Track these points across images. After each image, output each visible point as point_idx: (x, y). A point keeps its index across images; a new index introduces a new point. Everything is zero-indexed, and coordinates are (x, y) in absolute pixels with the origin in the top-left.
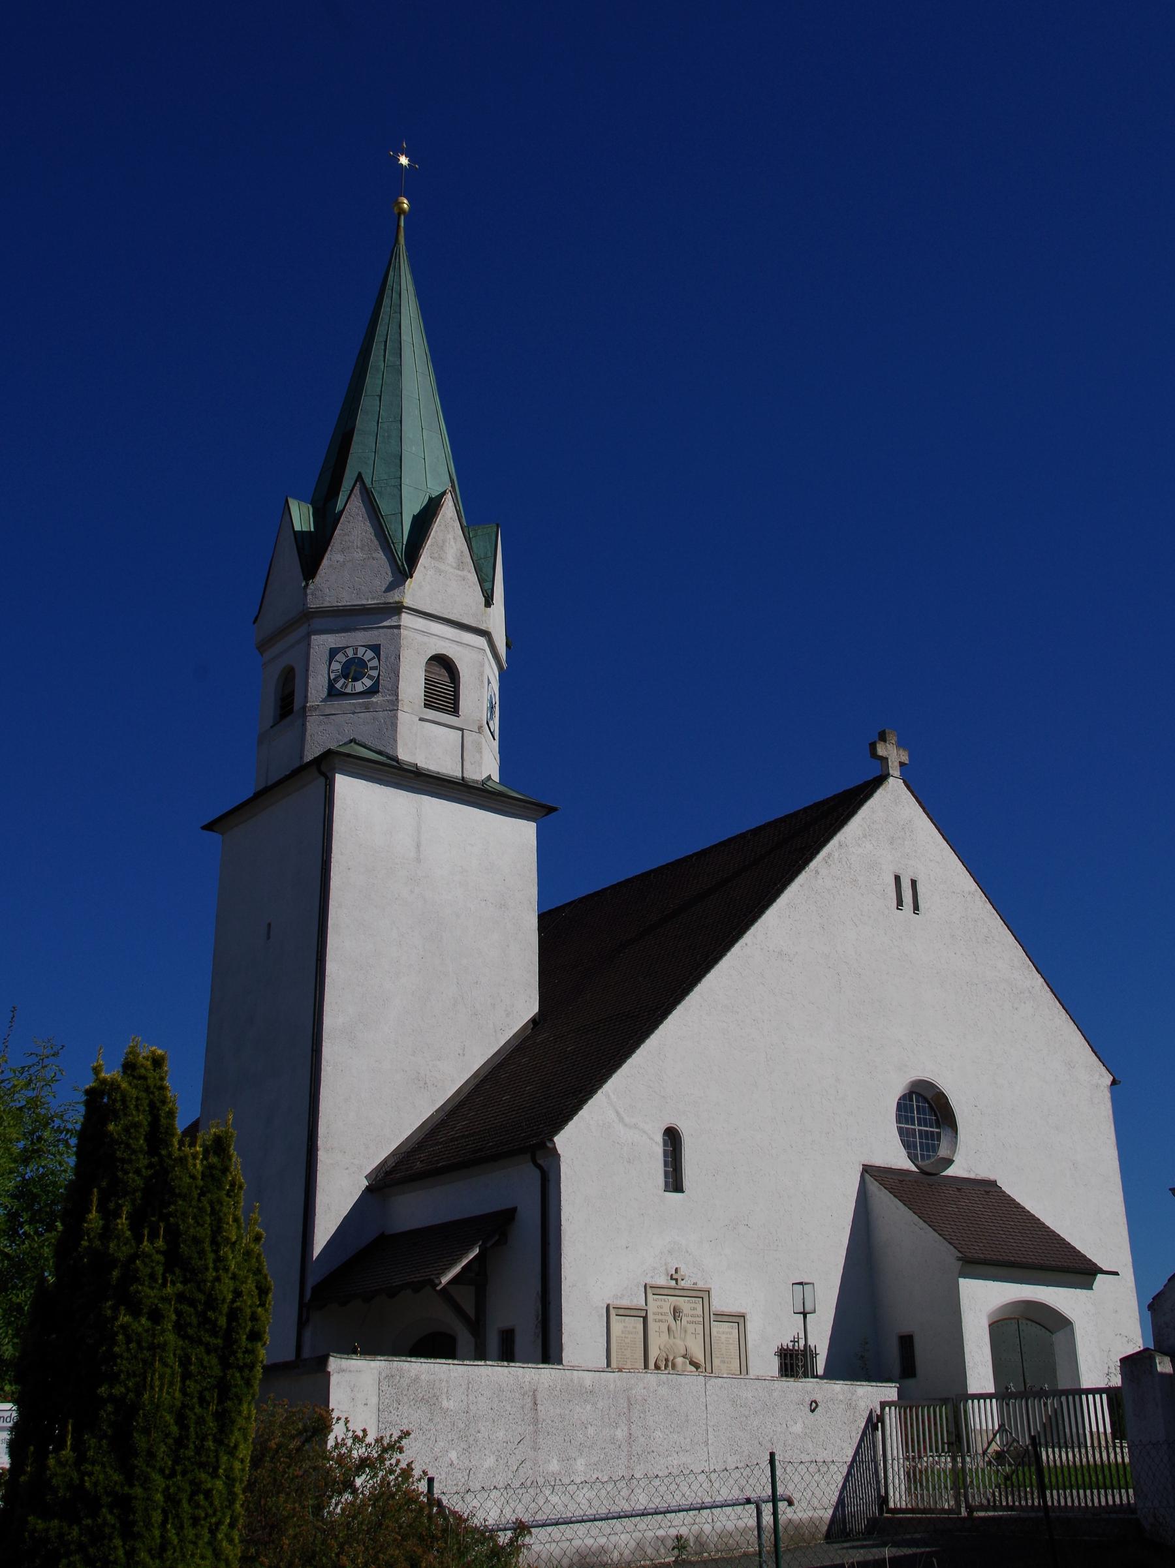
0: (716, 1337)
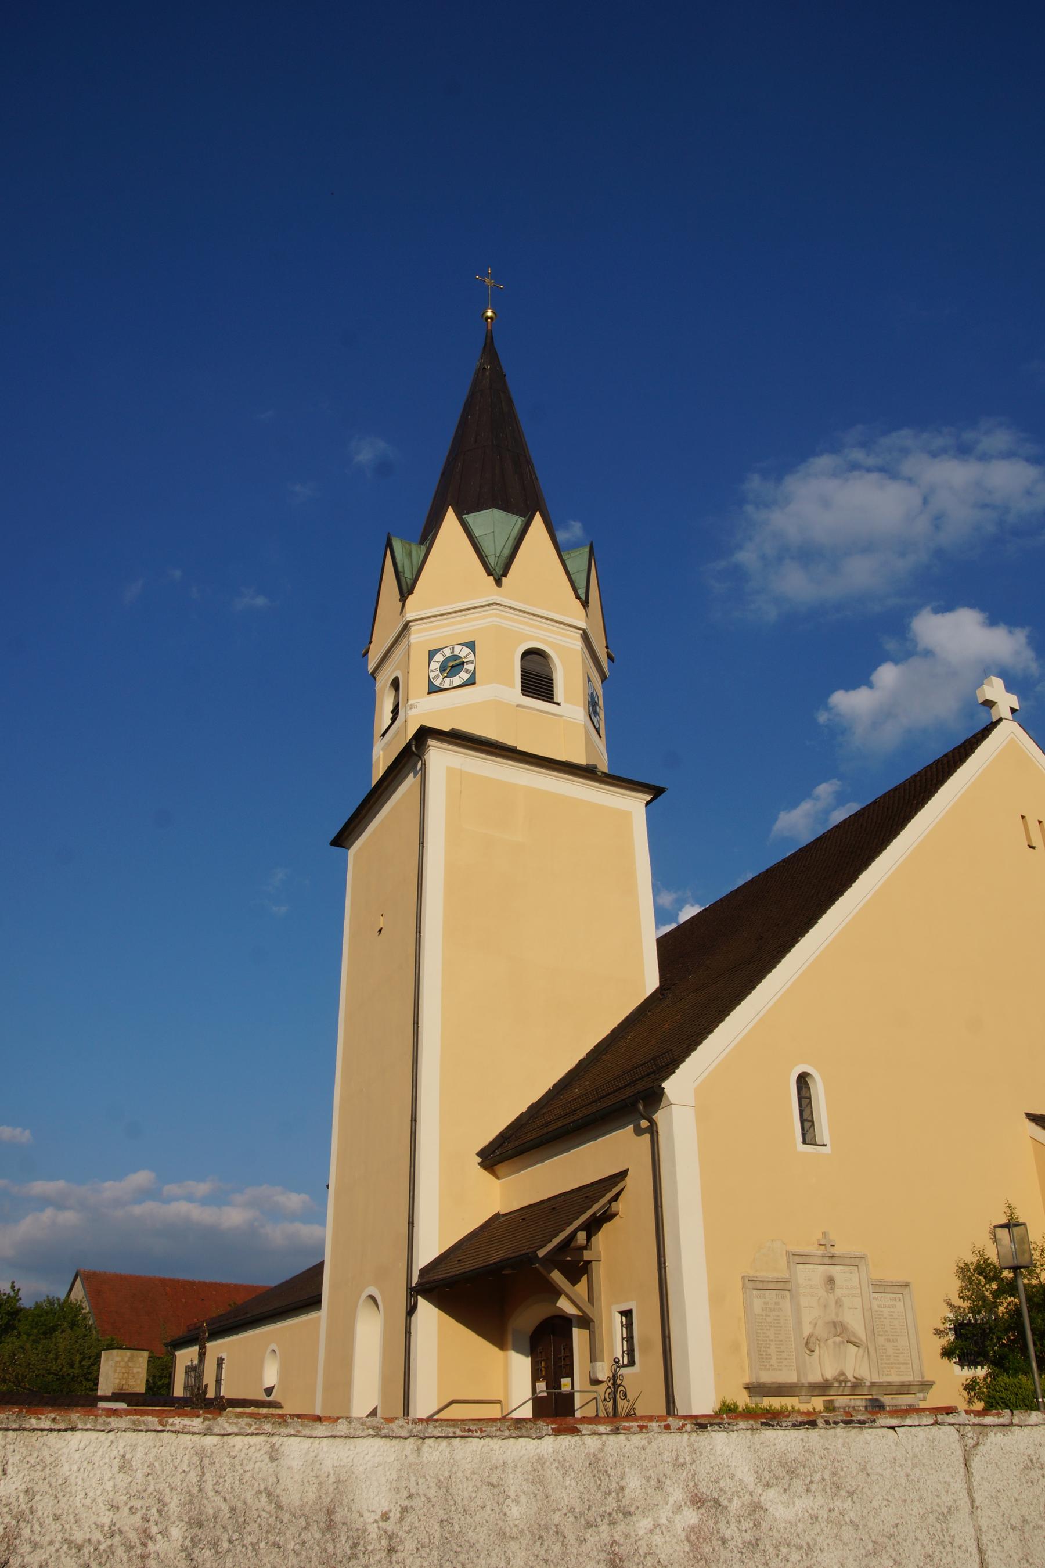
0: (877, 1311)
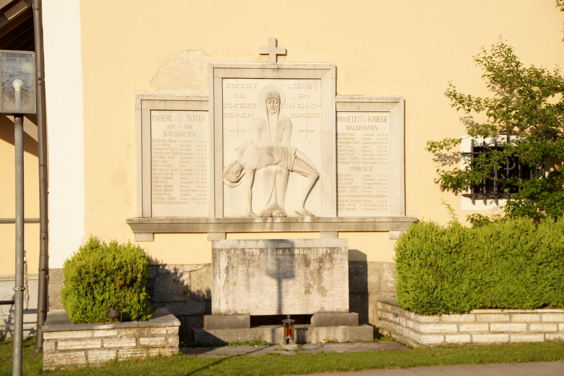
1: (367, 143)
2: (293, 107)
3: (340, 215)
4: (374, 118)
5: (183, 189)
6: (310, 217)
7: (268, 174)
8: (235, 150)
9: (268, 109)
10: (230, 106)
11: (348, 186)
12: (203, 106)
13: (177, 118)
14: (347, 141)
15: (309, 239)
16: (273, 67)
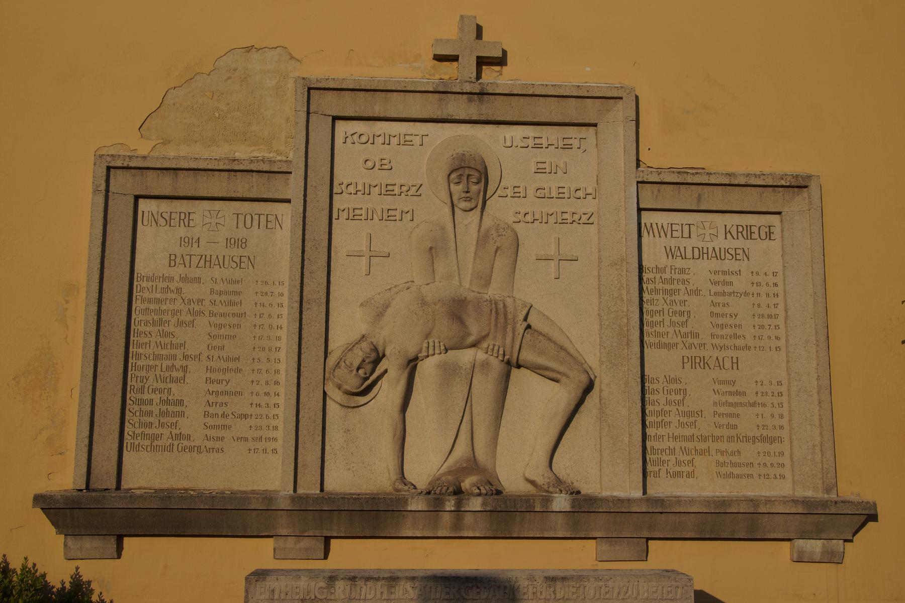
0: (662, 270)
1: (723, 294)
2: (522, 195)
3: (651, 492)
4: (740, 229)
5: (212, 410)
6: (568, 497)
7: (448, 372)
8: (362, 305)
9: (455, 198)
10: (352, 189)
11: (673, 408)
12: (276, 188)
13: (207, 220)
14: (668, 287)
15: (564, 579)
16: (467, 88)
